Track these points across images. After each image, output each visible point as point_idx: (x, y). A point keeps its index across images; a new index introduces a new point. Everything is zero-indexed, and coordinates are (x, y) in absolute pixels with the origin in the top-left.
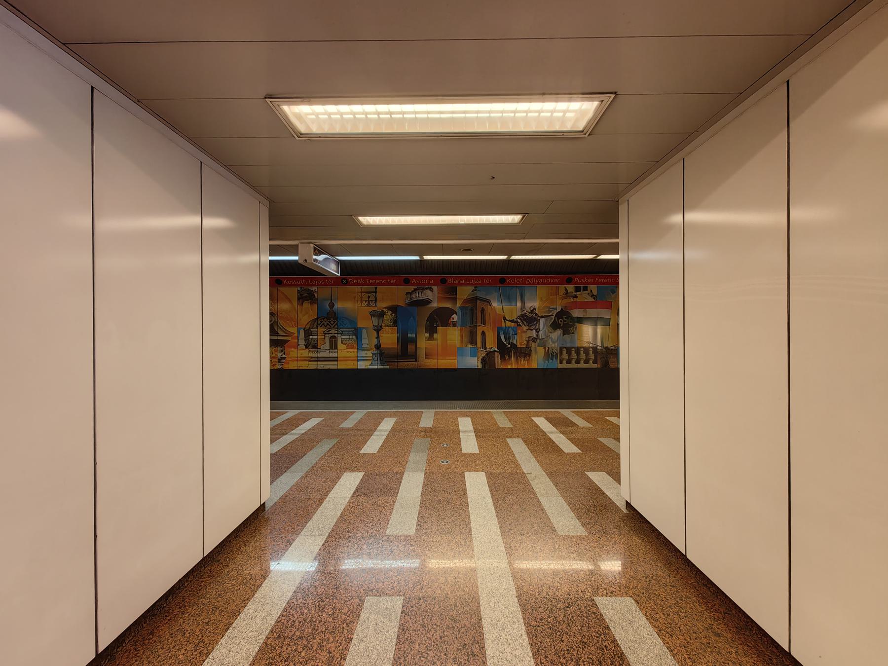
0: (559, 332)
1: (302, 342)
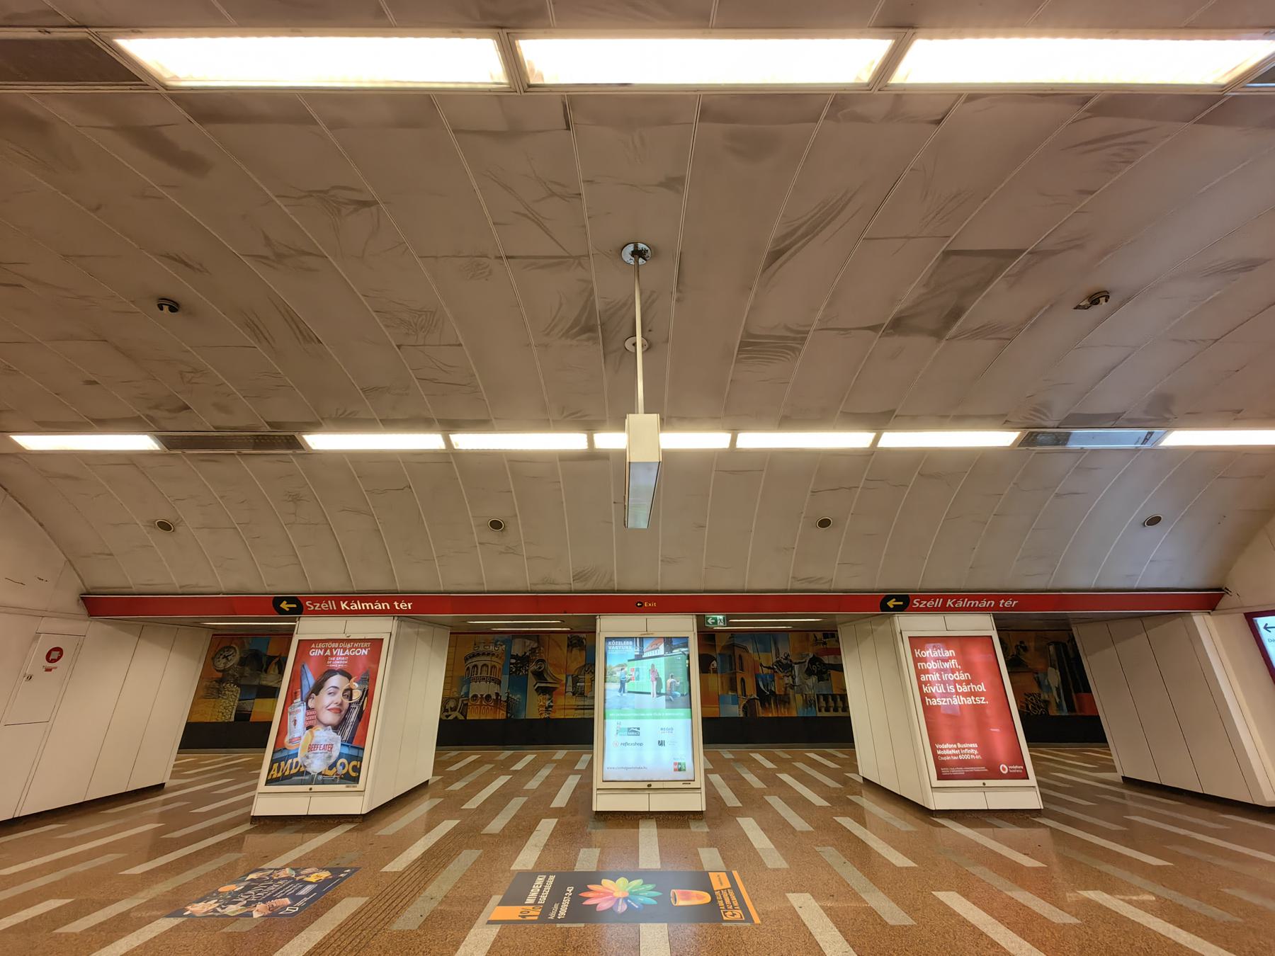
0: (814, 678)
1: (570, 689)
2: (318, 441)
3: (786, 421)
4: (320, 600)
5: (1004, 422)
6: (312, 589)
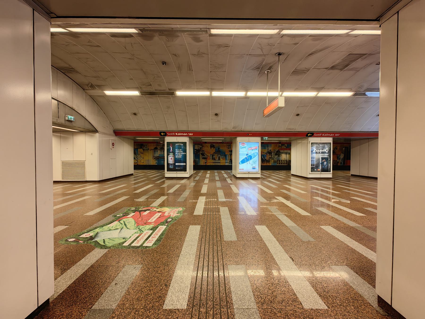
0: (277, 156)
2: (179, 93)
3: (297, 89)
4: (171, 133)
5: (350, 90)
6: (168, 130)
